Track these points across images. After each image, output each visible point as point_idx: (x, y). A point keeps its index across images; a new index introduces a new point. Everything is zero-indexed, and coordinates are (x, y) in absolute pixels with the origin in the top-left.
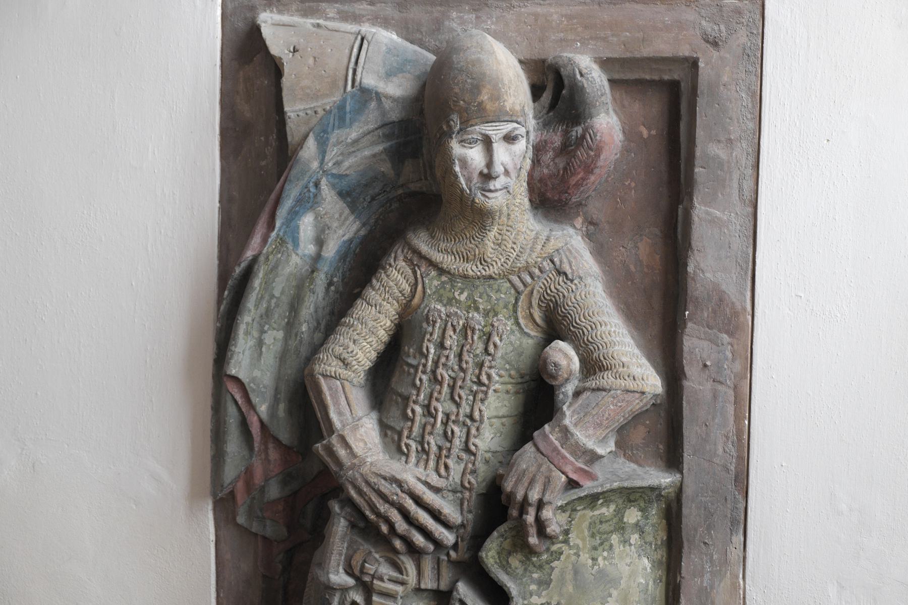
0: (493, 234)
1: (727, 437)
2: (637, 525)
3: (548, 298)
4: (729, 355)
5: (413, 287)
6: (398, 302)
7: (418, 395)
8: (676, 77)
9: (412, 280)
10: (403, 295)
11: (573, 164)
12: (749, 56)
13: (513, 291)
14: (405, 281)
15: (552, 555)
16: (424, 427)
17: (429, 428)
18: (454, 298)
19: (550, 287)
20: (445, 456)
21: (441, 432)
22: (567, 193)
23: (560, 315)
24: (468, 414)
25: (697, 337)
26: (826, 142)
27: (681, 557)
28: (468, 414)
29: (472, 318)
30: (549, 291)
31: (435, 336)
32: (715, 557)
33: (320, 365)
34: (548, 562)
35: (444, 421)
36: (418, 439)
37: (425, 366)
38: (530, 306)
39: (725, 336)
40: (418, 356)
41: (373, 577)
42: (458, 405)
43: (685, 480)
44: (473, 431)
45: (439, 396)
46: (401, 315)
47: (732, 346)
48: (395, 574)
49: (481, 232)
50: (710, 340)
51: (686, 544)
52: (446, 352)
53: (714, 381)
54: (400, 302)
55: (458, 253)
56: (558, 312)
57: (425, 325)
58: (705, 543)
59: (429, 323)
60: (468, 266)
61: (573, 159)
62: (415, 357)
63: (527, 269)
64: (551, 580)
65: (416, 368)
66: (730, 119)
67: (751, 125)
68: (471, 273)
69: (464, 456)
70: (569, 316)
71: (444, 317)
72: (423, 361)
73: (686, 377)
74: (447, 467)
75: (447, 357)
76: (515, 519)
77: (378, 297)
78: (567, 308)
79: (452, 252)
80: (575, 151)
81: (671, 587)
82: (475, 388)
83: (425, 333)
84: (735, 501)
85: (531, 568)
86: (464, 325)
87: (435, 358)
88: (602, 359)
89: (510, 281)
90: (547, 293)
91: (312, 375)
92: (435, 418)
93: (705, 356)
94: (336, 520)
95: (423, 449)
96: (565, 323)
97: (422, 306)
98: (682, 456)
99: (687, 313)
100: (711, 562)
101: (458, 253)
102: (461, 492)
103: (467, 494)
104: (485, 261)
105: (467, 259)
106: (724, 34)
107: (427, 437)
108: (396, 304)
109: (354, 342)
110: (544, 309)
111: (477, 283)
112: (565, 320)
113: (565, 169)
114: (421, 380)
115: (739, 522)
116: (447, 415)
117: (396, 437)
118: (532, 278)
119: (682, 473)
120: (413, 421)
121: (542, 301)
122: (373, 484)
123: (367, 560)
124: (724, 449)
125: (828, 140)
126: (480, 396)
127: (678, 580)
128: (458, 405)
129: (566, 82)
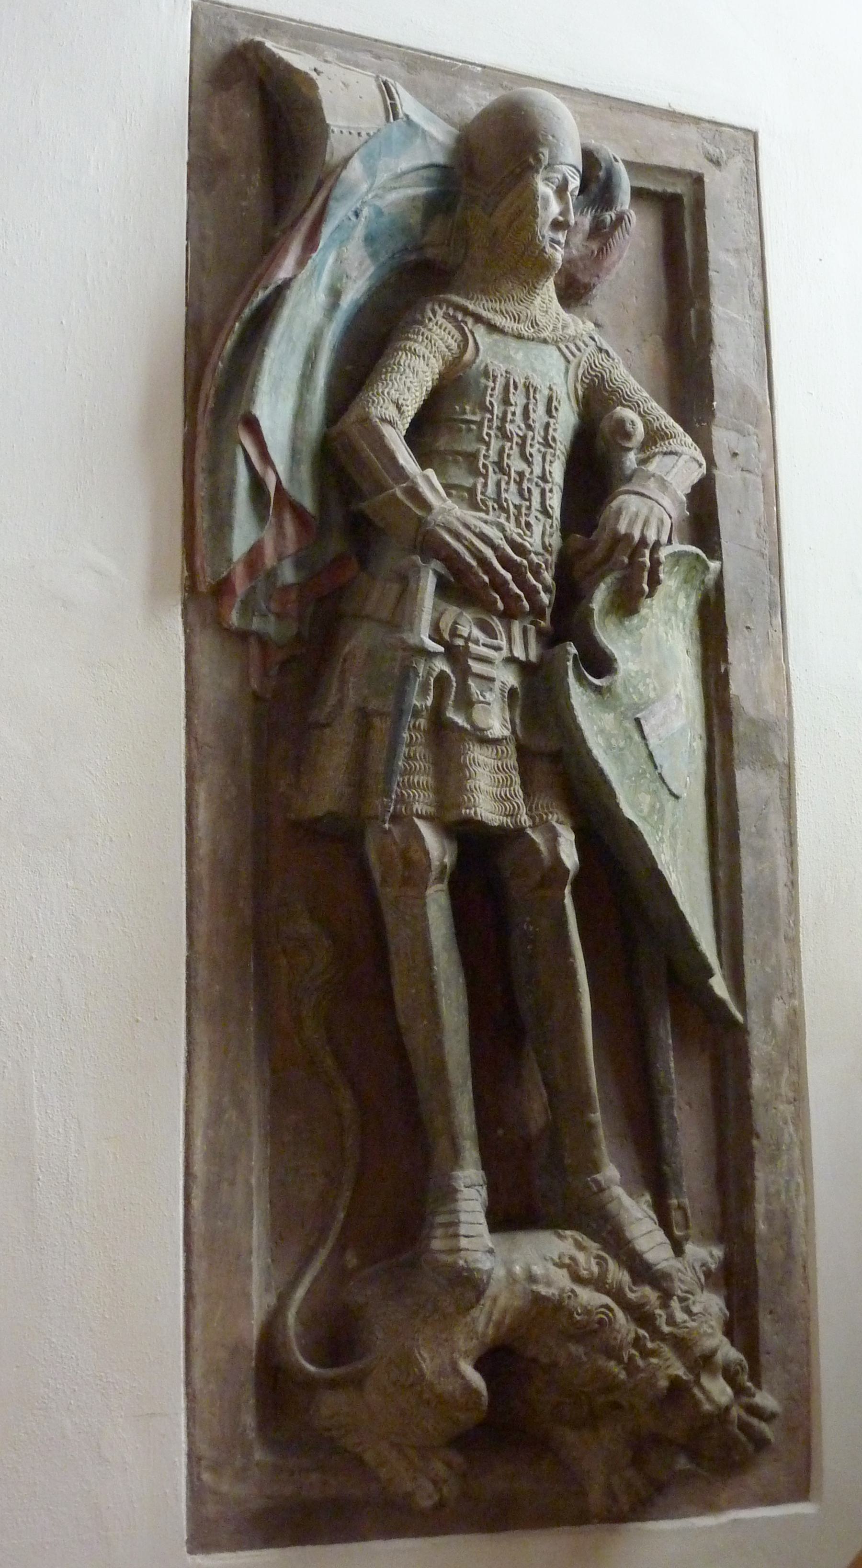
0: (539, 299)
1: (760, 524)
2: (682, 612)
3: (593, 373)
4: (756, 445)
5: (462, 344)
6: (443, 360)
7: (487, 450)
8: (679, 191)
9: (457, 335)
10: (450, 350)
11: (610, 244)
12: (746, 179)
13: (562, 360)
14: (450, 337)
15: (641, 620)
16: (498, 484)
17: (503, 486)
18: (510, 357)
19: (594, 362)
20: (525, 514)
21: (515, 491)
22: (598, 276)
23: (607, 391)
24: (540, 475)
25: (725, 427)
26: (818, 261)
27: (727, 643)
28: (540, 475)
29: (533, 377)
30: (593, 366)
31: (496, 392)
32: (758, 640)
33: (376, 408)
34: (638, 628)
35: (518, 479)
36: (492, 497)
37: (490, 420)
38: (576, 380)
39: (750, 427)
40: (477, 410)
41: (467, 639)
42: (529, 464)
43: (725, 565)
44: (548, 495)
45: (511, 452)
46: (442, 375)
47: (757, 436)
48: (489, 641)
49: (530, 295)
50: (738, 431)
51: (730, 630)
52: (512, 409)
53: (742, 470)
54: (446, 358)
55: (507, 313)
56: (604, 386)
57: (483, 381)
58: (748, 628)
59: (489, 377)
60: (521, 326)
61: (611, 240)
62: (474, 413)
63: (573, 339)
64: (641, 647)
65: (480, 424)
66: (735, 231)
67: (755, 239)
68: (526, 334)
69: (540, 516)
70: (620, 391)
71: (504, 374)
72: (488, 416)
73: (716, 466)
74: (528, 525)
75: (514, 414)
76: (624, 567)
77: (424, 349)
78: (615, 382)
79: (501, 311)
80: (611, 234)
81: (712, 681)
82: (543, 449)
83: (486, 387)
84: (771, 584)
85: (623, 633)
86: (525, 384)
87: (500, 415)
88: (663, 427)
89: (560, 349)
90: (591, 368)
91: (365, 420)
92: (509, 477)
93: (732, 445)
94: (422, 574)
95: (501, 508)
96: (614, 397)
97: (478, 361)
98: (720, 544)
99: (715, 403)
100: (755, 646)
101: (507, 313)
102: (542, 555)
103: (548, 556)
104: (537, 325)
105: (519, 320)
106: (725, 157)
107: (504, 495)
108: (441, 361)
109: (409, 389)
110: (586, 386)
111: (532, 344)
112: (615, 395)
113: (601, 250)
114: (488, 435)
115: (777, 604)
116: (521, 474)
117: (466, 495)
118: (579, 350)
119: (720, 559)
120: (486, 476)
121: (586, 377)
122: (473, 527)
123: (458, 621)
124: (758, 536)
125: (821, 260)
126: (548, 458)
127: (723, 670)
128: (529, 464)
129: (603, 165)
